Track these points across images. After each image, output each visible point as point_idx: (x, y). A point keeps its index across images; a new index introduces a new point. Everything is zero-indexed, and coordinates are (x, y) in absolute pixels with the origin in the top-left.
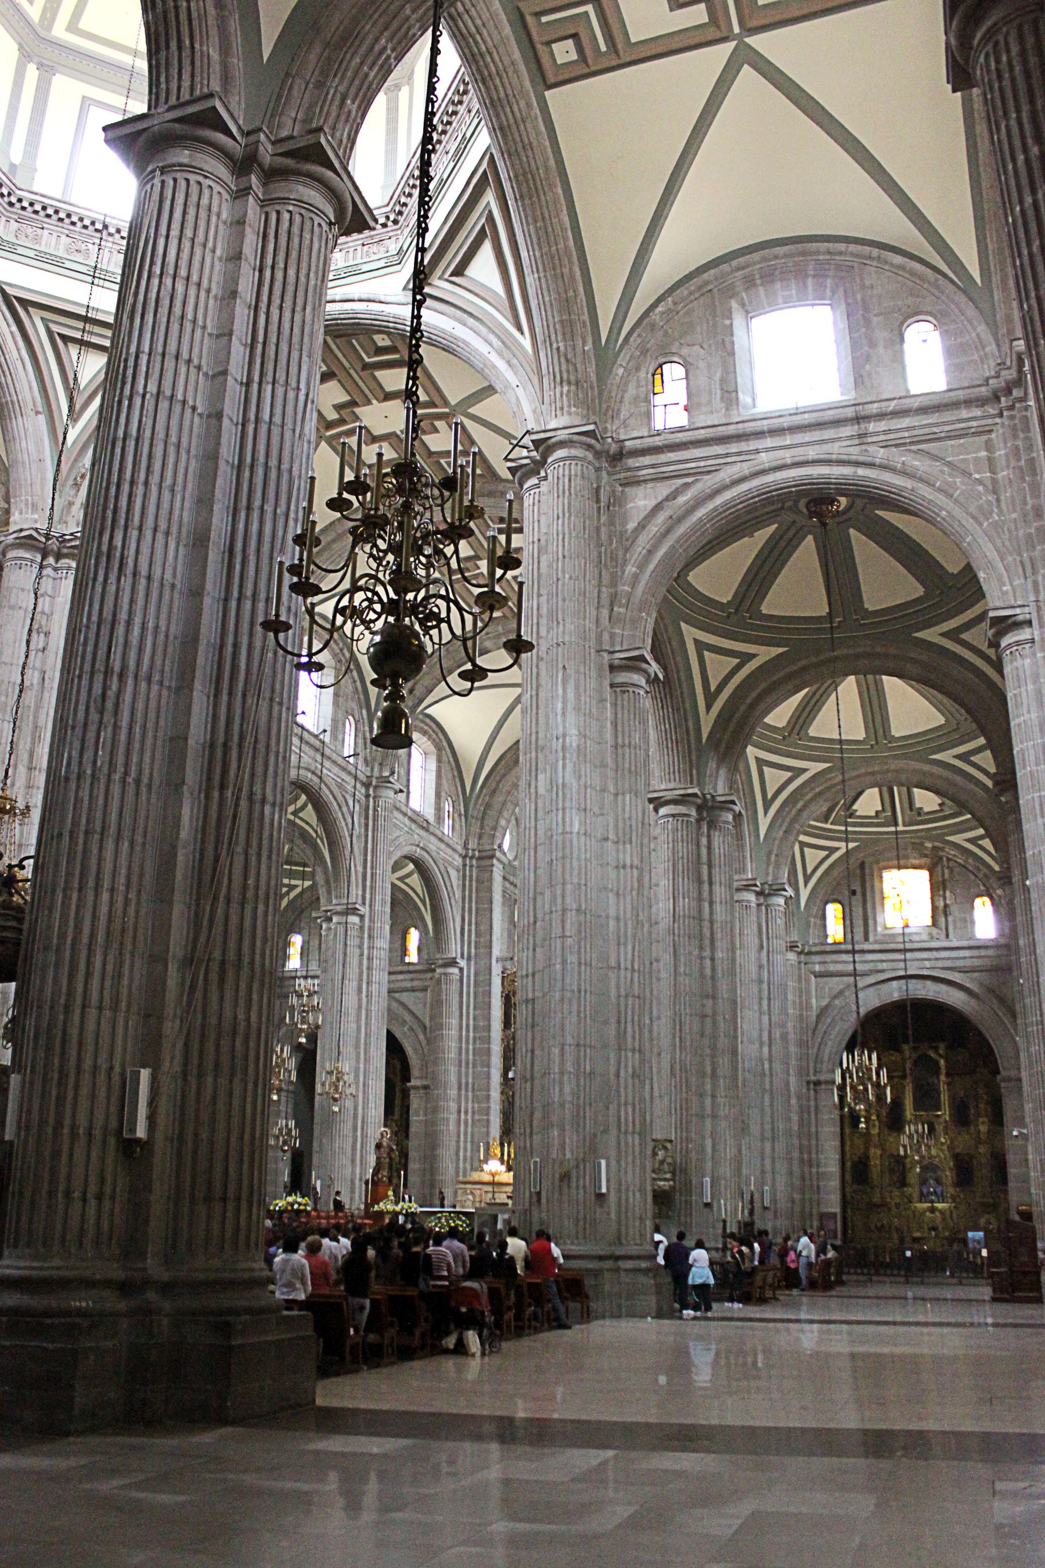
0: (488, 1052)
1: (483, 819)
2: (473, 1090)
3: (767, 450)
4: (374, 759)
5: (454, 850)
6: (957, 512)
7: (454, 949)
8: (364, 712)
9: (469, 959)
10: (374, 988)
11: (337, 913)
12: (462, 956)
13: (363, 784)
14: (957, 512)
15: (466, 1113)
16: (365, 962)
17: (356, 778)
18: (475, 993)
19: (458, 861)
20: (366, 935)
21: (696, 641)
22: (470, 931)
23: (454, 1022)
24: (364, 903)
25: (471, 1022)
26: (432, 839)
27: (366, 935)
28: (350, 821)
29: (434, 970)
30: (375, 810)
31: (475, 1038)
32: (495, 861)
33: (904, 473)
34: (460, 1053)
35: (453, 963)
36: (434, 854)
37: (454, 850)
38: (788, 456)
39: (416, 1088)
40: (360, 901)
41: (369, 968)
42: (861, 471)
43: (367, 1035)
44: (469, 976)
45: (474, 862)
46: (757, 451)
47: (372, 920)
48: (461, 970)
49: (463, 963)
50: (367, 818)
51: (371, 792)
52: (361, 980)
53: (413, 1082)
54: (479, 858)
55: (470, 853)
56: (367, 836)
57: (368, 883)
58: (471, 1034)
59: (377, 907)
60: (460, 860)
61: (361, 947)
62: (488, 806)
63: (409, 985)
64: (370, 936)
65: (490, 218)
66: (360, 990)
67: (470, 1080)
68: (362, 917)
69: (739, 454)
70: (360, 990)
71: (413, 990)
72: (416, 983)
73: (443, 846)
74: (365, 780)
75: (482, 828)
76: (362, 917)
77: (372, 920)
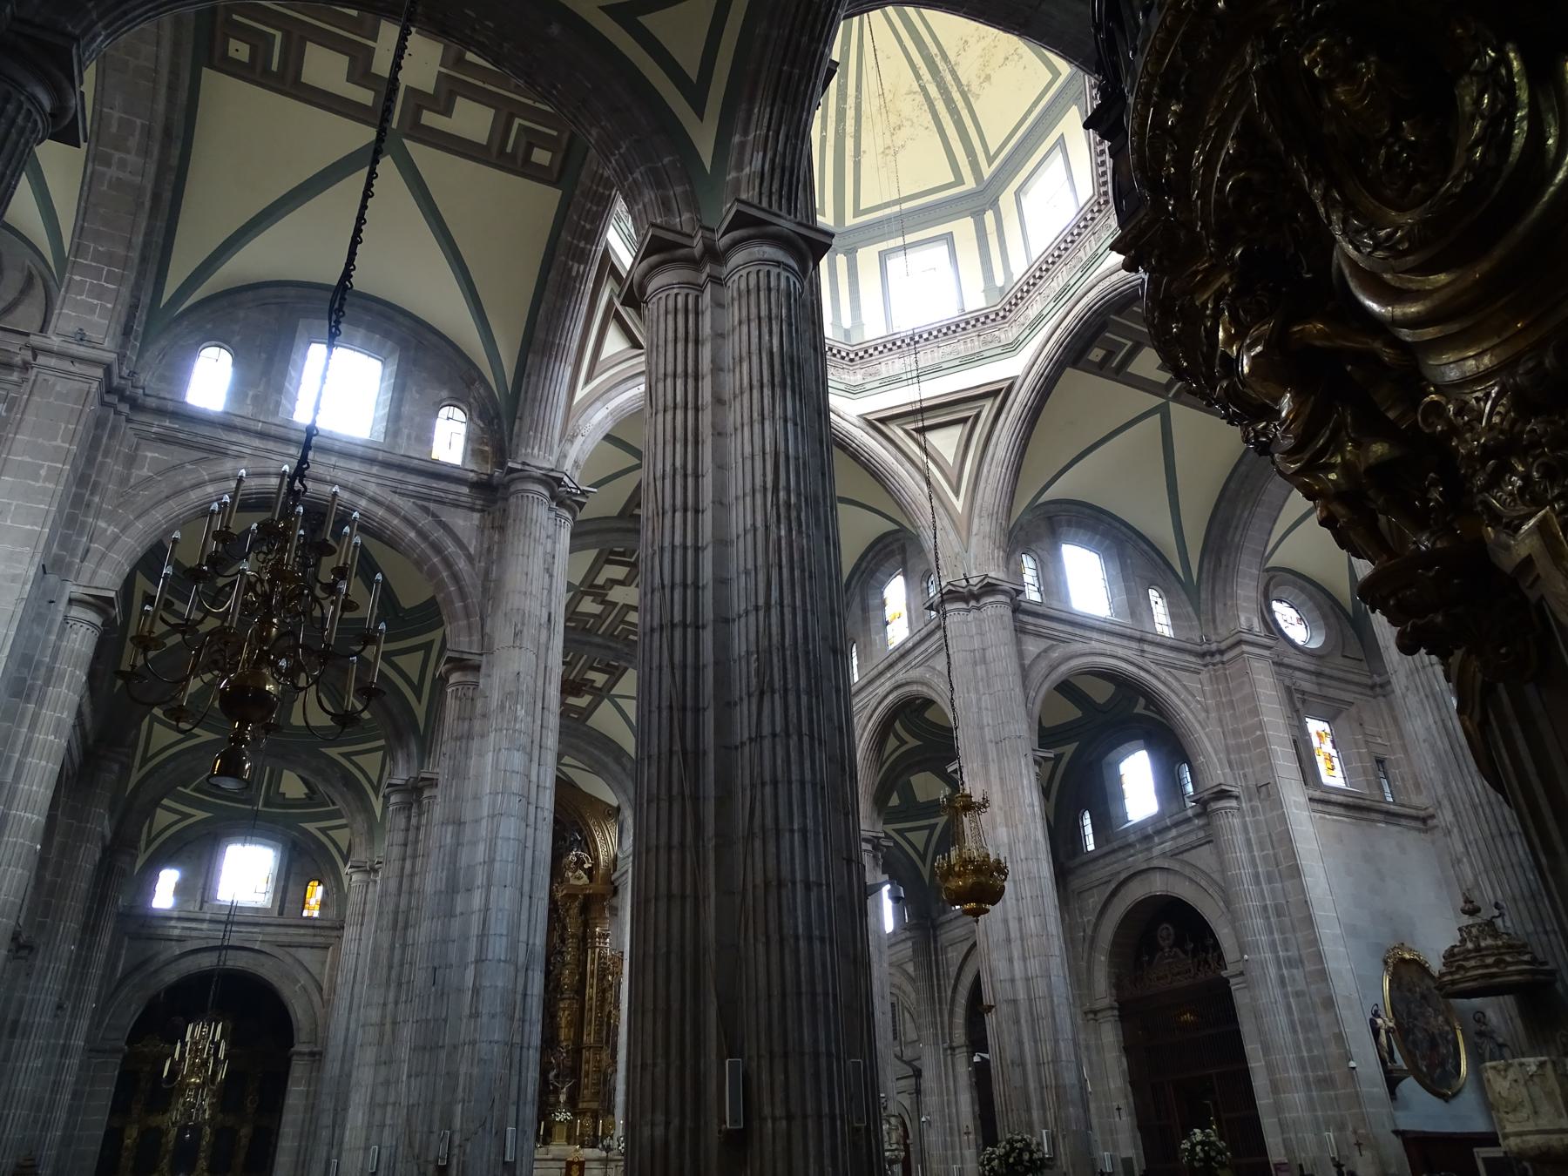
3: (1097, 640)
6: (1190, 716)
14: (1190, 716)
21: (432, 642)
33: (1164, 683)
38: (1108, 649)
39: (300, 1054)
42: (1143, 674)
46: (1091, 639)
53: (297, 1048)
63: (309, 940)
65: (977, 416)
69: (1081, 637)
71: (312, 947)
72: (319, 940)
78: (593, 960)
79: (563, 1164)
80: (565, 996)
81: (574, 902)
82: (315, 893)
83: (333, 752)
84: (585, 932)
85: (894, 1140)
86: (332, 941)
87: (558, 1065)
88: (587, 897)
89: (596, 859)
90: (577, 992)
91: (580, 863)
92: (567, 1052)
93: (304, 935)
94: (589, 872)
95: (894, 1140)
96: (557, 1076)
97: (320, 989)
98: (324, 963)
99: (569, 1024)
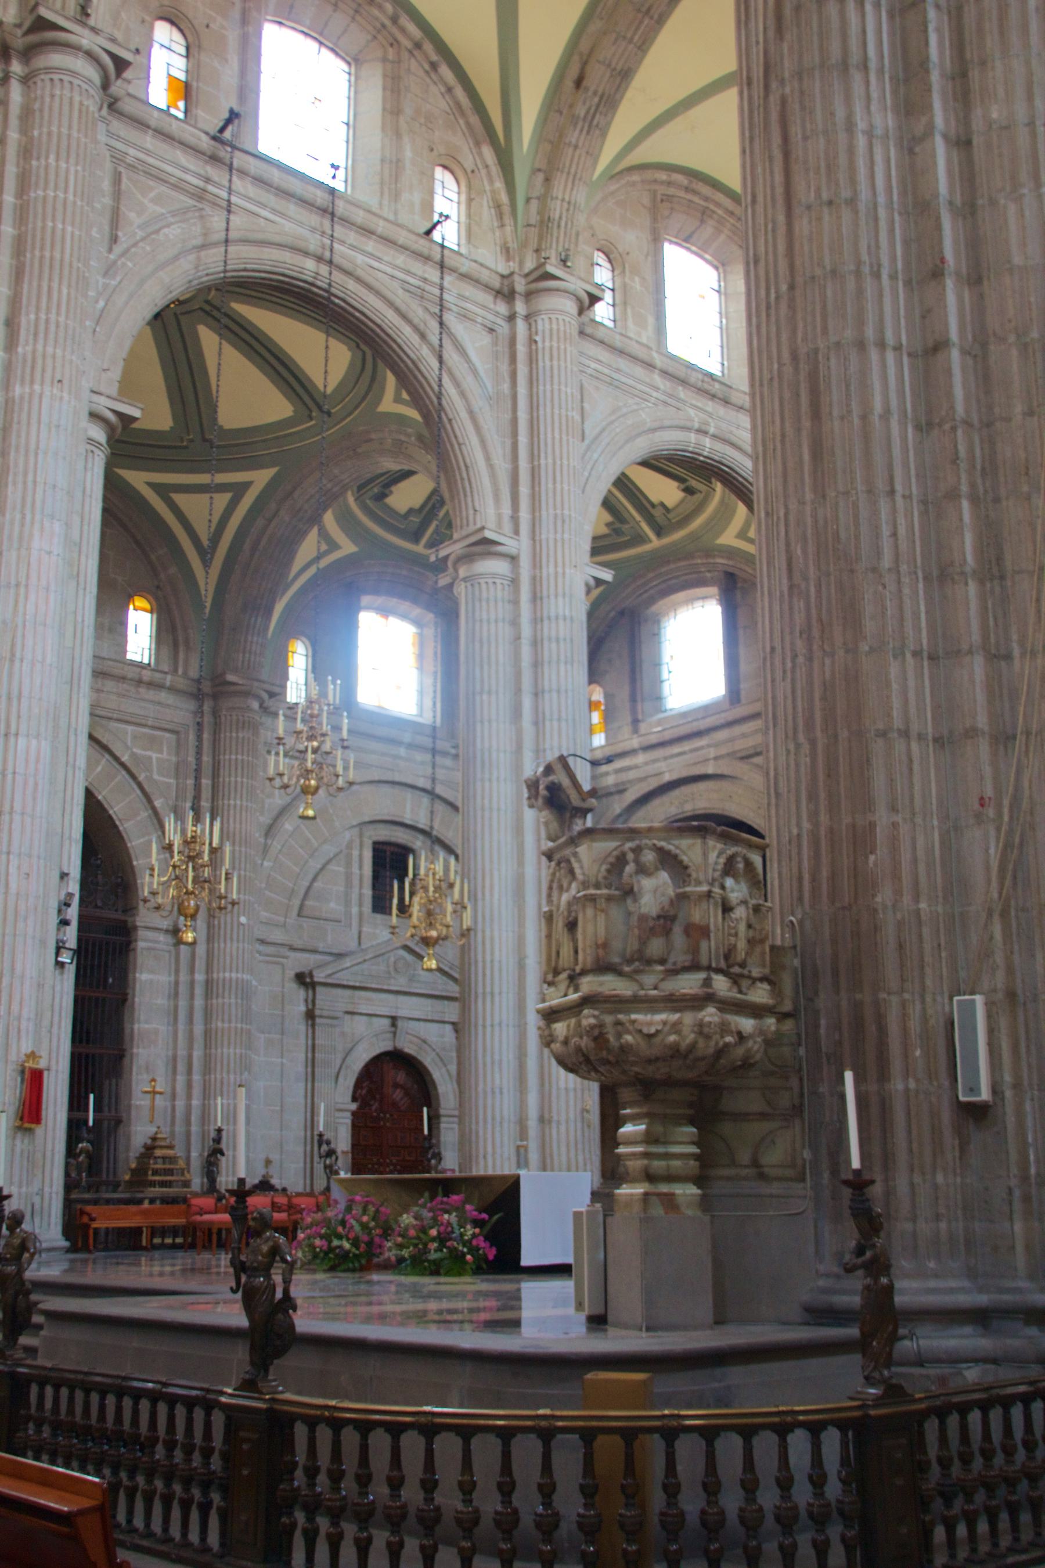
4: (524, 245)
8: (488, 152)
13: (498, 293)
24: (517, 532)
40: (507, 527)
41: (537, 664)
47: (536, 562)
52: (518, 691)
57: (524, 490)
61: (515, 623)
66: (517, 713)
70: (517, 713)
74: (496, 283)
76: (513, 559)
77: (536, 562)
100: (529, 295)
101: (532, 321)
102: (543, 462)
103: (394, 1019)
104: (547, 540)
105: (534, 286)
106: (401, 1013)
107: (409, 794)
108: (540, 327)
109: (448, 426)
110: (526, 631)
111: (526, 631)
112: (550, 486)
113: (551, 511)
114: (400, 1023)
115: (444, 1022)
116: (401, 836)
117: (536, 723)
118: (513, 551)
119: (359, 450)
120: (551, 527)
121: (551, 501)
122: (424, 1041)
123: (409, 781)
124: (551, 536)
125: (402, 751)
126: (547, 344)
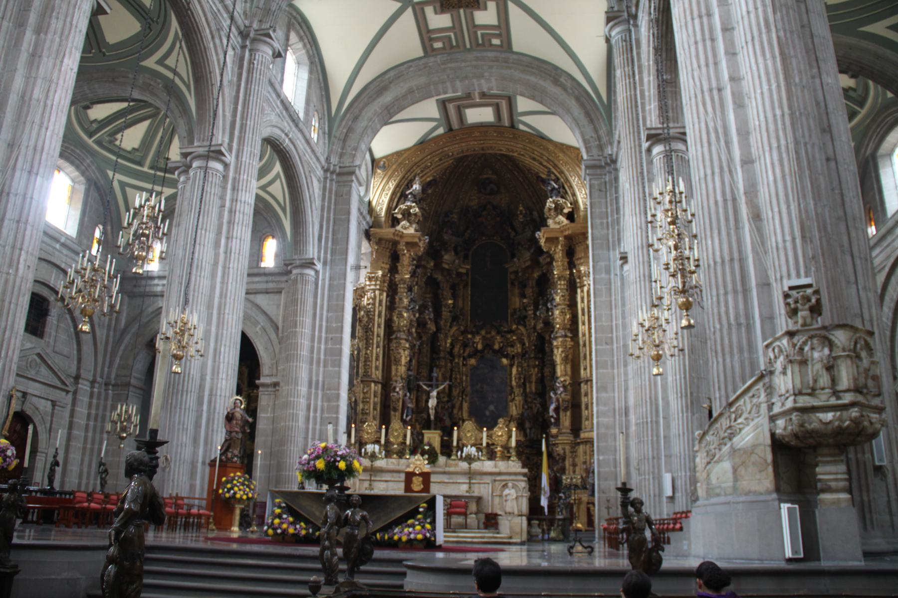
0: (340, 352)
1: (345, 141)
2: (323, 389)
5: (318, 159)
7: (312, 251)
9: (325, 264)
10: (235, 244)
11: (199, 157)
12: (319, 259)
13: (241, 33)
15: (315, 411)
16: (226, 214)
17: (232, 18)
18: (329, 297)
19: (320, 173)
20: (229, 186)
22: (327, 238)
23: (308, 321)
25: (324, 324)
26: (300, 136)
27: (229, 186)
28: (221, 57)
29: (290, 272)
30: (251, 62)
31: (326, 339)
32: (354, 178)
34: (312, 352)
35: (310, 264)
36: (300, 151)
37: (318, 159)
41: (231, 222)
43: (223, 295)
44: (324, 280)
45: (334, 177)
48: (317, 272)
49: (319, 266)
50: (241, 67)
51: (248, 43)
52: (219, 233)
53: (263, 380)
54: (339, 174)
55: (332, 169)
56: (239, 86)
57: (237, 133)
58: (324, 335)
59: (245, 158)
60: (322, 172)
61: (222, 198)
62: (350, 130)
63: (263, 286)
64: (233, 189)
66: (217, 244)
67: (321, 379)
68: (226, 166)
70: (217, 244)
71: (267, 292)
72: (271, 285)
73: (309, 150)
75: (343, 149)
77: (238, 171)
78: (582, 298)
79: (403, 477)
80: (559, 335)
81: (557, 246)
82: (271, 247)
83: (150, 63)
84: (571, 274)
85: (845, 382)
86: (283, 285)
87: (558, 400)
88: (568, 238)
89: (575, 203)
90: (571, 330)
91: (558, 209)
92: (564, 387)
93: (258, 282)
94: (571, 217)
95: (845, 382)
96: (557, 410)
97: (276, 328)
98: (278, 306)
99: (565, 360)
100: (254, 40)
101: (253, 53)
102: (248, 122)
103: (25, 394)
104: (245, 162)
105: (259, 37)
106: (30, 391)
107: (55, 271)
108: (257, 57)
109: (210, 87)
110: (228, 204)
111: (228, 204)
112: (251, 135)
113: (249, 149)
114: (28, 397)
115: (47, 399)
116: (45, 292)
117: (226, 253)
118: (228, 162)
119: (116, 80)
120: (248, 156)
121: (250, 144)
122: (37, 409)
123: (58, 263)
124: (248, 161)
125: (58, 246)
126: (259, 67)
